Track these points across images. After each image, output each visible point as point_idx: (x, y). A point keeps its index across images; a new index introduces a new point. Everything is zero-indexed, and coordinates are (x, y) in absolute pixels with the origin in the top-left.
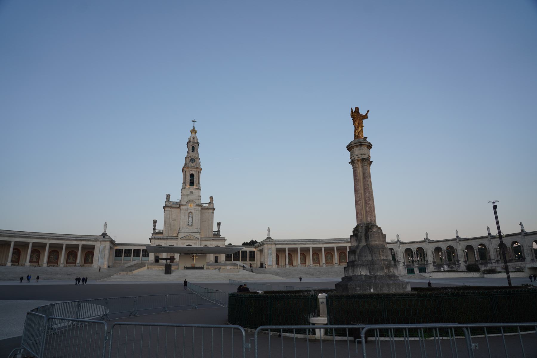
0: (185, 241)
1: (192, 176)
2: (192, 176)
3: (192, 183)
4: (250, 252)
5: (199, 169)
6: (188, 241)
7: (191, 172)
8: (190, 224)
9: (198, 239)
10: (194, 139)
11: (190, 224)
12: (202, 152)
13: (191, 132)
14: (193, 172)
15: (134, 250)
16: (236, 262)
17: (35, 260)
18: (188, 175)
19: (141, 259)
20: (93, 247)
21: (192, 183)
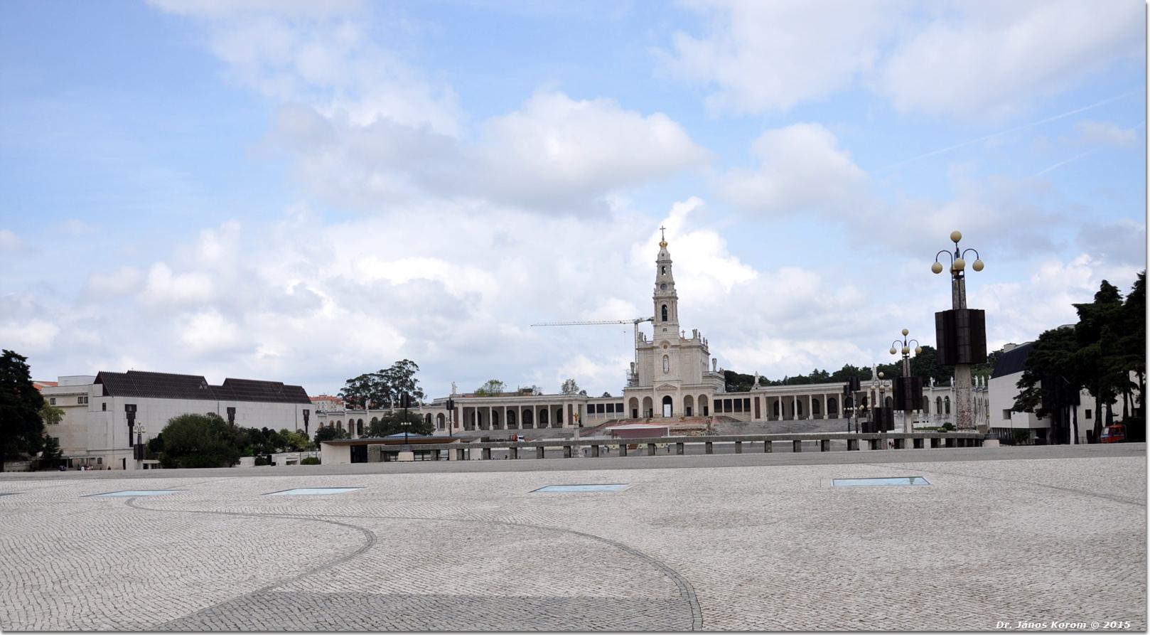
0: (660, 392)
1: (664, 306)
2: (664, 306)
3: (665, 318)
4: (745, 399)
5: (674, 298)
6: (665, 392)
7: (663, 304)
8: (666, 370)
9: (675, 389)
10: (663, 255)
11: (666, 370)
12: (676, 273)
13: (661, 245)
14: (666, 303)
15: (607, 405)
16: (728, 414)
17: (511, 421)
18: (660, 307)
19: (615, 415)
20: (562, 406)
21: (665, 318)
